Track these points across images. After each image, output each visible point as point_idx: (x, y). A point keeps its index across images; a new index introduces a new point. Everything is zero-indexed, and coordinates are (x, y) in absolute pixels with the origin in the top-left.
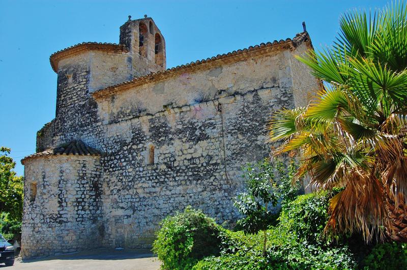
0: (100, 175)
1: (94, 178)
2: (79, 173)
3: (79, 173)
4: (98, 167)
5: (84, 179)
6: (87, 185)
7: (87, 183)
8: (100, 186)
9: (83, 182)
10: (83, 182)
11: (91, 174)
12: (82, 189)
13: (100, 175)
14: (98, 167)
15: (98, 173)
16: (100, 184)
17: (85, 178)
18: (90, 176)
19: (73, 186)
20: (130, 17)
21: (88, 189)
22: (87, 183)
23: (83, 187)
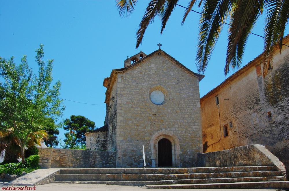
0: (106, 141)
1: (103, 142)
2: (97, 140)
3: (97, 140)
4: (105, 137)
5: (99, 143)
6: (100, 146)
7: (100, 145)
8: (106, 146)
9: (98, 144)
10: (98, 144)
11: (102, 140)
12: (98, 147)
13: (106, 141)
14: (105, 137)
15: (105, 140)
16: (106, 145)
17: (99, 142)
18: (101, 141)
19: (94, 146)
20: (128, 57)
21: (100, 147)
22: (100, 145)
23: (98, 146)
